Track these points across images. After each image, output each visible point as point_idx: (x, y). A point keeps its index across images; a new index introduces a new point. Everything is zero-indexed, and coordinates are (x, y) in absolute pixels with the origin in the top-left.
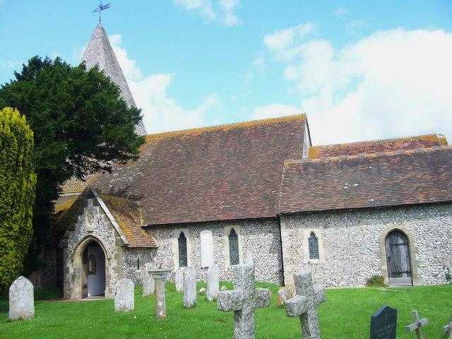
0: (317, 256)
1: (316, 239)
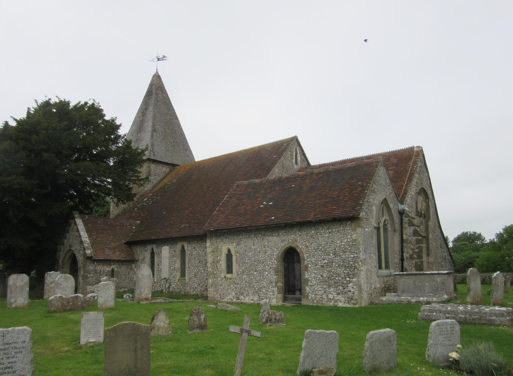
0: (232, 273)
1: (231, 255)
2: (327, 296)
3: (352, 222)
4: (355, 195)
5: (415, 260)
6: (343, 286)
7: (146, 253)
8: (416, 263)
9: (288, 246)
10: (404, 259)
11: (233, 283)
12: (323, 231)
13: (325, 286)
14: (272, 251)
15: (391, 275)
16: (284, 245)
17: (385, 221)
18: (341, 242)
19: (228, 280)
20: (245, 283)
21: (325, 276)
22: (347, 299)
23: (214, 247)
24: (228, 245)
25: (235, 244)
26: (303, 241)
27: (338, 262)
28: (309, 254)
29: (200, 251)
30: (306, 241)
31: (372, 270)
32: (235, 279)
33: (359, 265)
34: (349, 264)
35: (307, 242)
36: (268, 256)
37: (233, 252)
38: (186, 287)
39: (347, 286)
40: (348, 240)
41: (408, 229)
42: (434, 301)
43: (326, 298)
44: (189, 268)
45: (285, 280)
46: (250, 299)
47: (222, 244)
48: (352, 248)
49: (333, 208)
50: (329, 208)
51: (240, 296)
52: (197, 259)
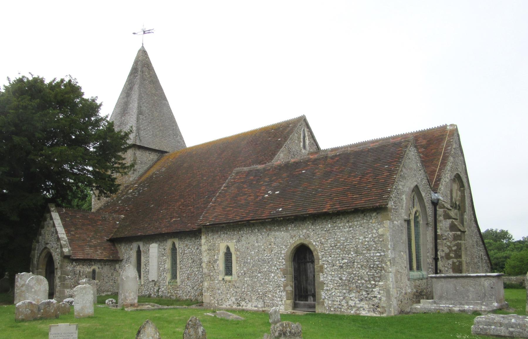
1: (231, 254)
2: (347, 303)
3: (377, 214)
4: (380, 181)
5: (452, 260)
6: (367, 291)
7: (131, 252)
8: (454, 263)
9: (298, 243)
10: (438, 259)
11: (233, 286)
12: (342, 225)
13: (344, 291)
14: (279, 249)
15: (423, 277)
16: (294, 241)
17: (416, 213)
18: (365, 238)
19: (227, 283)
20: (247, 286)
21: (344, 278)
22: (372, 306)
23: (210, 244)
24: (227, 242)
25: (234, 241)
26: (317, 237)
27: (360, 262)
28: (325, 253)
29: (194, 249)
30: (321, 237)
31: (402, 271)
32: (236, 282)
33: (387, 265)
34: (374, 265)
35: (321, 238)
36: (275, 255)
37: (232, 250)
38: (178, 291)
39: (372, 291)
40: (372, 236)
41: (444, 222)
42: (483, 310)
43: (345, 305)
44: (181, 269)
45: (295, 284)
46: (253, 306)
47: (219, 241)
48: (379, 245)
49: (355, 196)
50: (349, 197)
51: (241, 301)
52: (190, 259)
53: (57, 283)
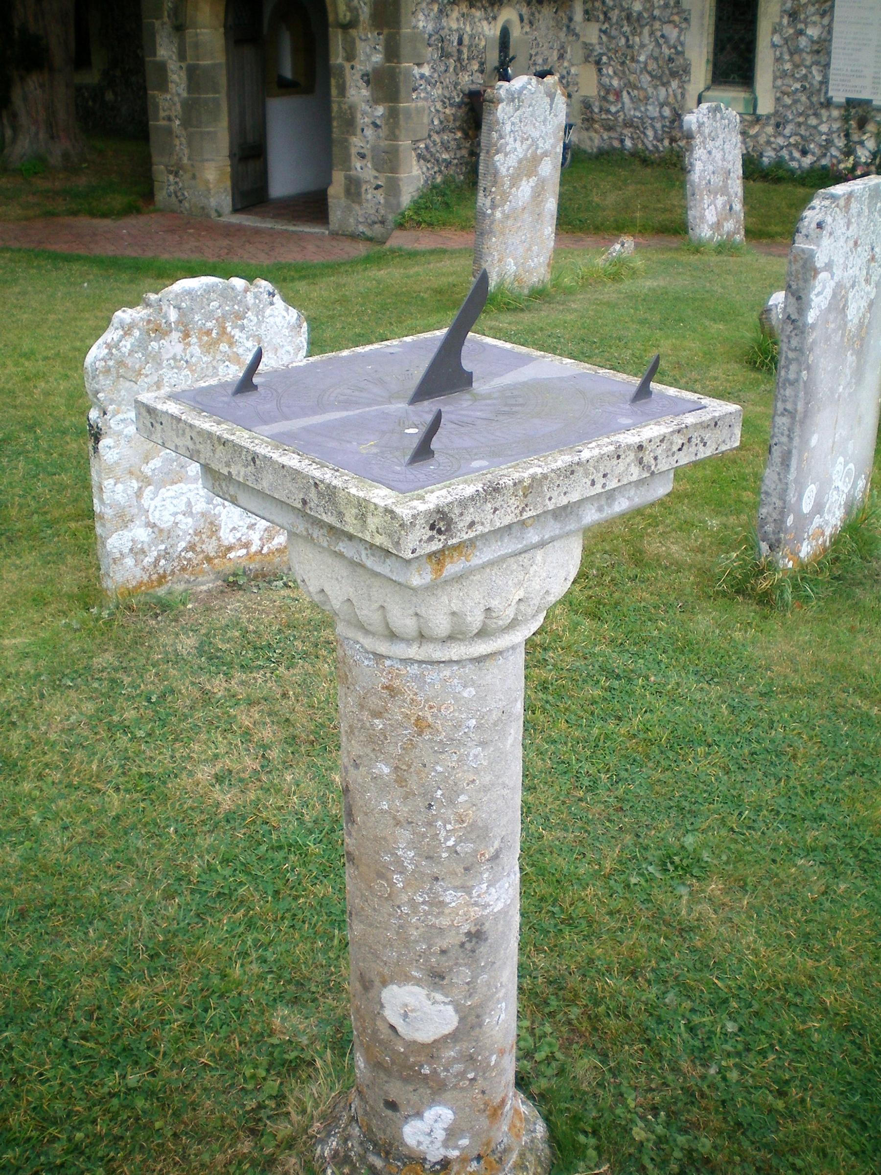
53: (352, 108)
